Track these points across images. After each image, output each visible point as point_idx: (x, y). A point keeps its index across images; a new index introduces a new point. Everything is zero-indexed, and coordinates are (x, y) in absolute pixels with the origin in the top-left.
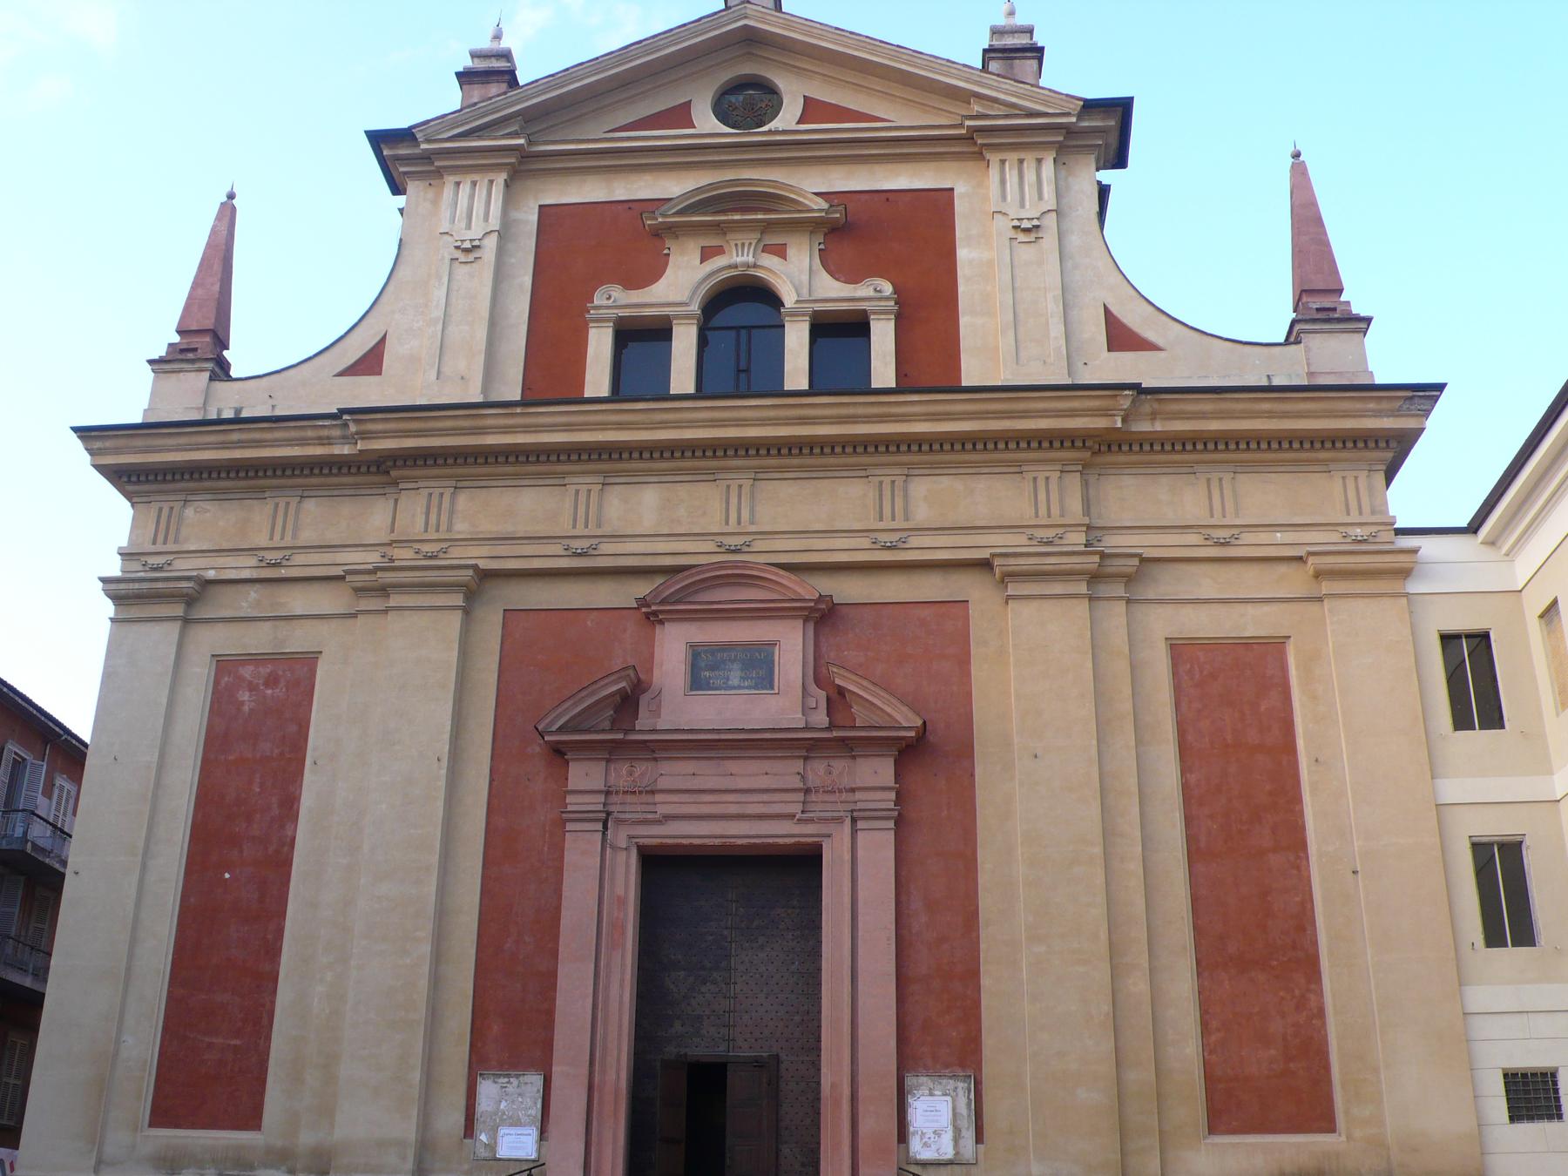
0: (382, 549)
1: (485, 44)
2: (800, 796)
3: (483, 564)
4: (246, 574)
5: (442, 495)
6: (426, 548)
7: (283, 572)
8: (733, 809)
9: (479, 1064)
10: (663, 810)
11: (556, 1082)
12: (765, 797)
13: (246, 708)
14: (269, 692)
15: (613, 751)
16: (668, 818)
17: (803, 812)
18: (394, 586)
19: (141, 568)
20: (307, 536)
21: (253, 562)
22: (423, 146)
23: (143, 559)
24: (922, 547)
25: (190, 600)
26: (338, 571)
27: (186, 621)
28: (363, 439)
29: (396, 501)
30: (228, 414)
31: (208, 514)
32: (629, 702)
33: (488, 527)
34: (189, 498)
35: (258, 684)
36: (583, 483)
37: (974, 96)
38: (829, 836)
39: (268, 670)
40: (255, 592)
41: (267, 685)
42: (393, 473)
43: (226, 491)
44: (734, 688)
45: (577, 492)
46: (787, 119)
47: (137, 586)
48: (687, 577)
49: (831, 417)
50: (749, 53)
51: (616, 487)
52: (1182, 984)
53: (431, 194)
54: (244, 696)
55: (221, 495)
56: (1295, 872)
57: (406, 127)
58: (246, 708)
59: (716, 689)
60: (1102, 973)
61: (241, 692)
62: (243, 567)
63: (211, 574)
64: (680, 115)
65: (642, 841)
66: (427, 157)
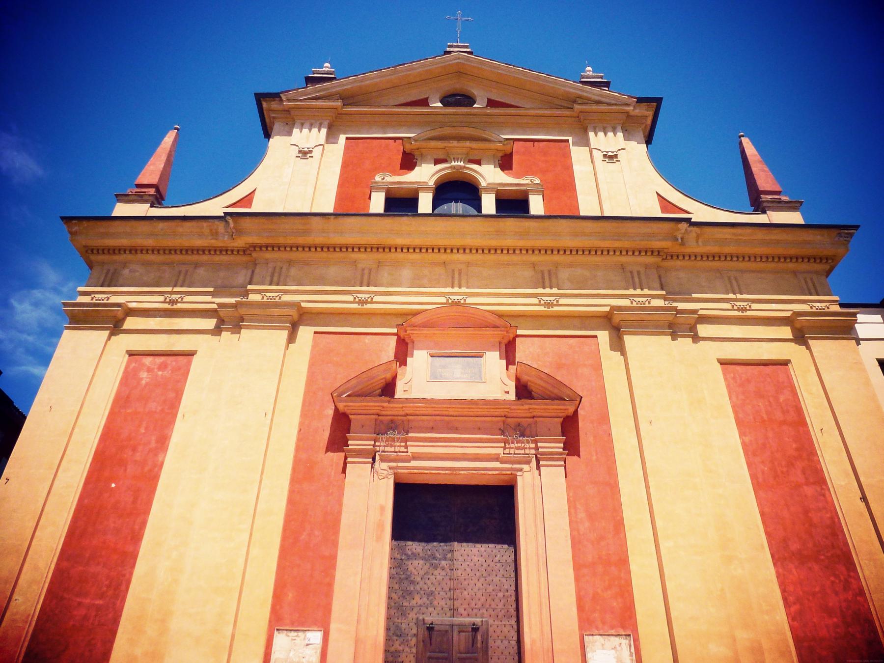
2: (503, 445)
10: (411, 450)
13: (144, 382)
14: (160, 373)
16: (416, 457)
17: (504, 454)
35: (153, 369)
38: (521, 470)
41: (159, 369)
54: (144, 375)
56: (822, 498)
58: (144, 382)
64: (424, 102)
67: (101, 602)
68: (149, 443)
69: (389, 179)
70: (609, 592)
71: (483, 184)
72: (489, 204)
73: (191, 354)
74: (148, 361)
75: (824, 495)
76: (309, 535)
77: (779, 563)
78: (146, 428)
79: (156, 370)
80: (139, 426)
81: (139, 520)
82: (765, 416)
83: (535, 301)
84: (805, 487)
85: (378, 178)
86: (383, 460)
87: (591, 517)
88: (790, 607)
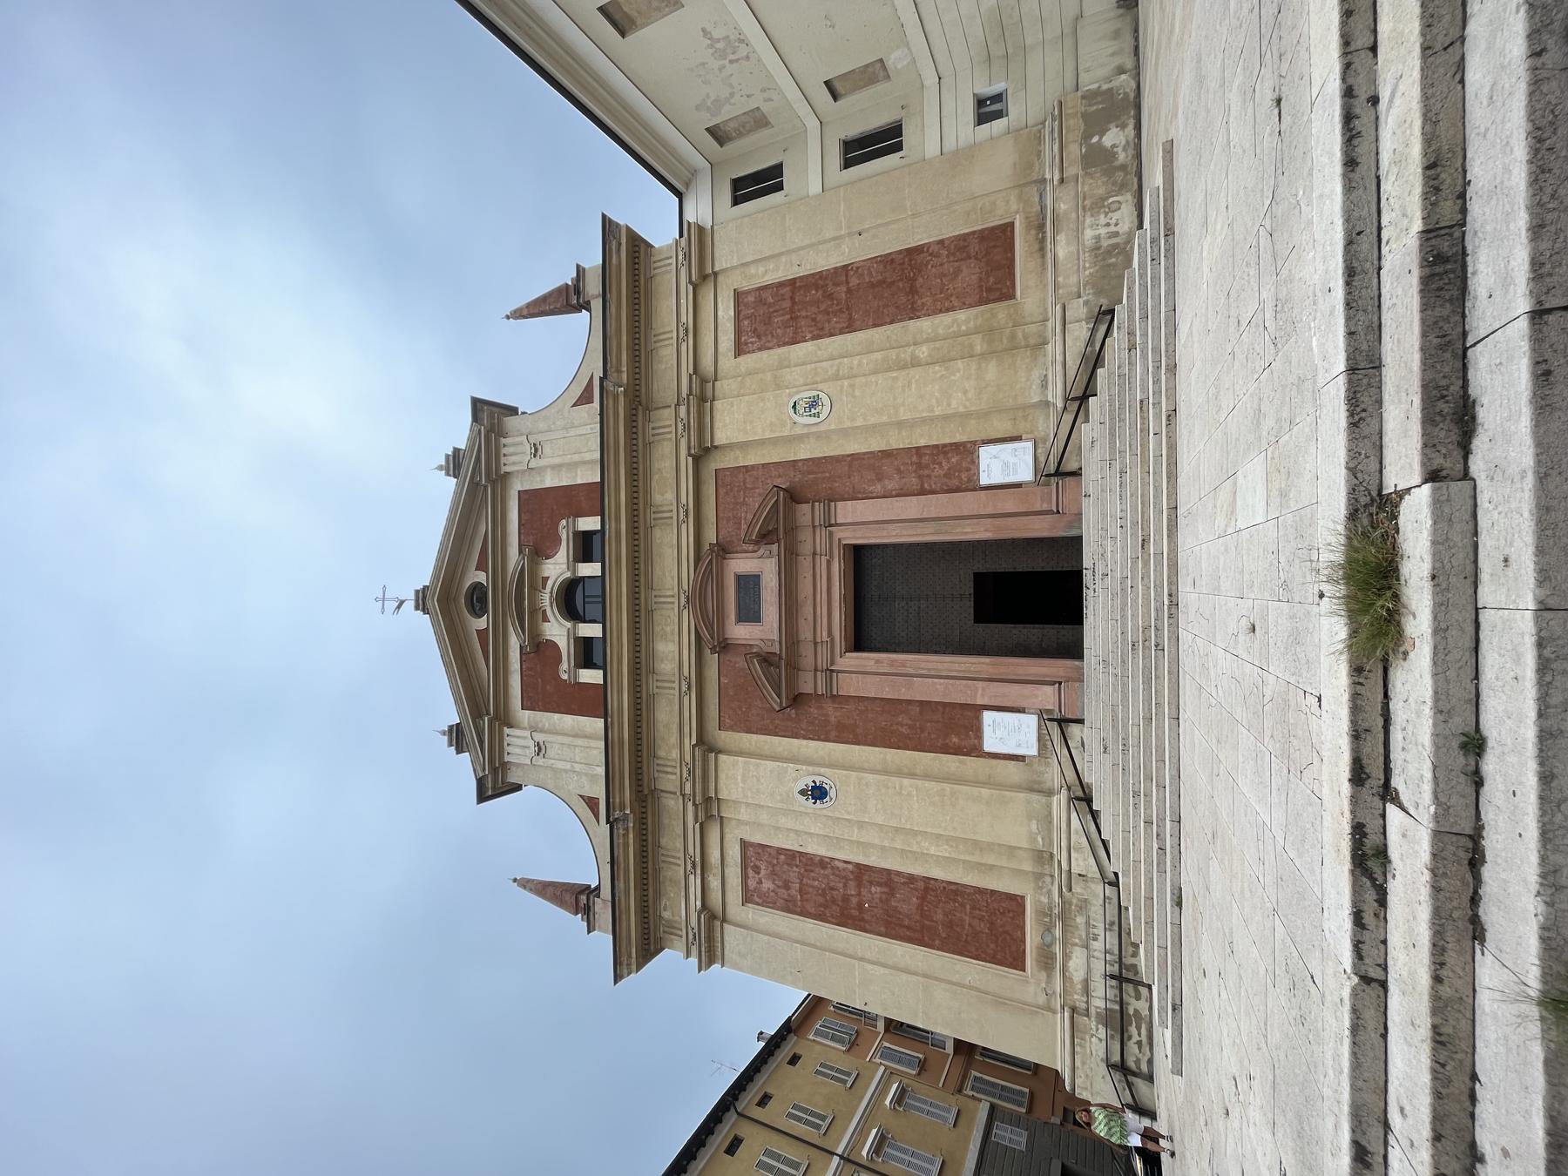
0: (686, 800)
1: (446, 738)
2: (817, 557)
3: (694, 742)
5: (658, 765)
6: (685, 775)
7: (698, 859)
8: (825, 596)
9: (976, 750)
10: (825, 638)
11: (986, 701)
14: (763, 872)
15: (794, 667)
16: (830, 634)
21: (692, 877)
24: (687, 497)
25: (712, 917)
27: (724, 920)
29: (662, 791)
32: (767, 660)
33: (674, 739)
41: (758, 873)
42: (646, 792)
43: (655, 891)
45: (657, 687)
52: (924, 325)
53: (513, 769)
55: (658, 894)
60: (916, 373)
63: (699, 903)
65: (843, 650)
66: (494, 771)
67: (968, 907)
68: (826, 876)
69: (564, 666)
70: (944, 464)
71: (568, 574)
72: (590, 569)
73: (744, 844)
74: (752, 883)
75: (858, 268)
76: (902, 725)
77: (918, 314)
78: (814, 879)
80: (812, 887)
81: (896, 879)
82: (788, 317)
83: (684, 526)
84: (851, 285)
85: (565, 677)
86: (832, 663)
87: (880, 478)
88: (953, 307)
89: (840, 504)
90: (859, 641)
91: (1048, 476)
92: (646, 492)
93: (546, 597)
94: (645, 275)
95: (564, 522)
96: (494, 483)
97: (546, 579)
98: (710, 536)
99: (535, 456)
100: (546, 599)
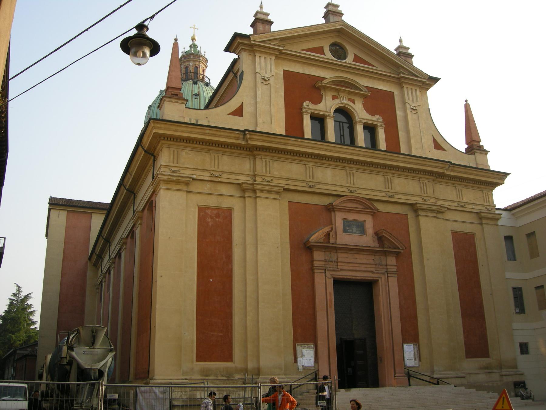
4: (207, 178)
6: (267, 178)
7: (219, 180)
8: (358, 269)
12: (366, 266)
14: (217, 219)
18: (258, 190)
19: (169, 171)
20: (226, 168)
22: (252, 42)
23: (170, 168)
25: (187, 184)
26: (240, 182)
28: (250, 140)
30: (194, 122)
31: (190, 155)
33: (285, 174)
34: (183, 148)
36: (310, 164)
37: (401, 67)
39: (216, 212)
40: (209, 185)
44: (354, 233)
46: (350, 59)
47: (171, 178)
48: (345, 198)
49: (349, 153)
50: (338, 35)
51: (319, 167)
54: (209, 220)
57: (248, 34)
58: (210, 224)
59: (350, 233)
61: (208, 219)
62: (205, 176)
63: (195, 177)
65: (335, 276)
66: (252, 46)
71: (357, 119)
79: (215, 218)
89: (396, 279)
90: (338, 282)
91: (408, 372)
92: (399, 175)
93: (345, 101)
94: (483, 188)
95: (381, 120)
96: (399, 79)
97: (353, 101)
98: (381, 207)
99: (412, 108)
100: (345, 101)
